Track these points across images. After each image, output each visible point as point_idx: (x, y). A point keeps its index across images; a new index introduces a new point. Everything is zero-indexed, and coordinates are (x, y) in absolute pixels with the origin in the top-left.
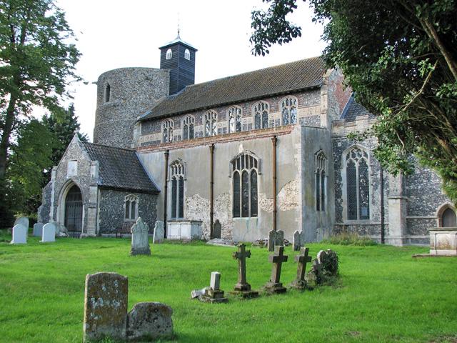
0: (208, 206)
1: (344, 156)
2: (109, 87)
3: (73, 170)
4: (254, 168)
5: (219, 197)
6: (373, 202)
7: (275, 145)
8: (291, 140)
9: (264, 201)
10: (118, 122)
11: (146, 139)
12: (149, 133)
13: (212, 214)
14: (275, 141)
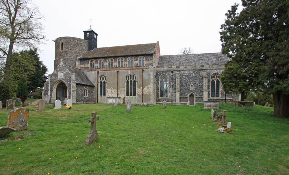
0: (116, 92)
1: (160, 77)
2: (62, 44)
3: (61, 76)
4: (135, 79)
5: (120, 89)
6: (169, 92)
7: (143, 72)
8: (149, 71)
9: (138, 91)
10: (68, 58)
11: (82, 66)
12: (83, 64)
13: (118, 95)
14: (143, 71)
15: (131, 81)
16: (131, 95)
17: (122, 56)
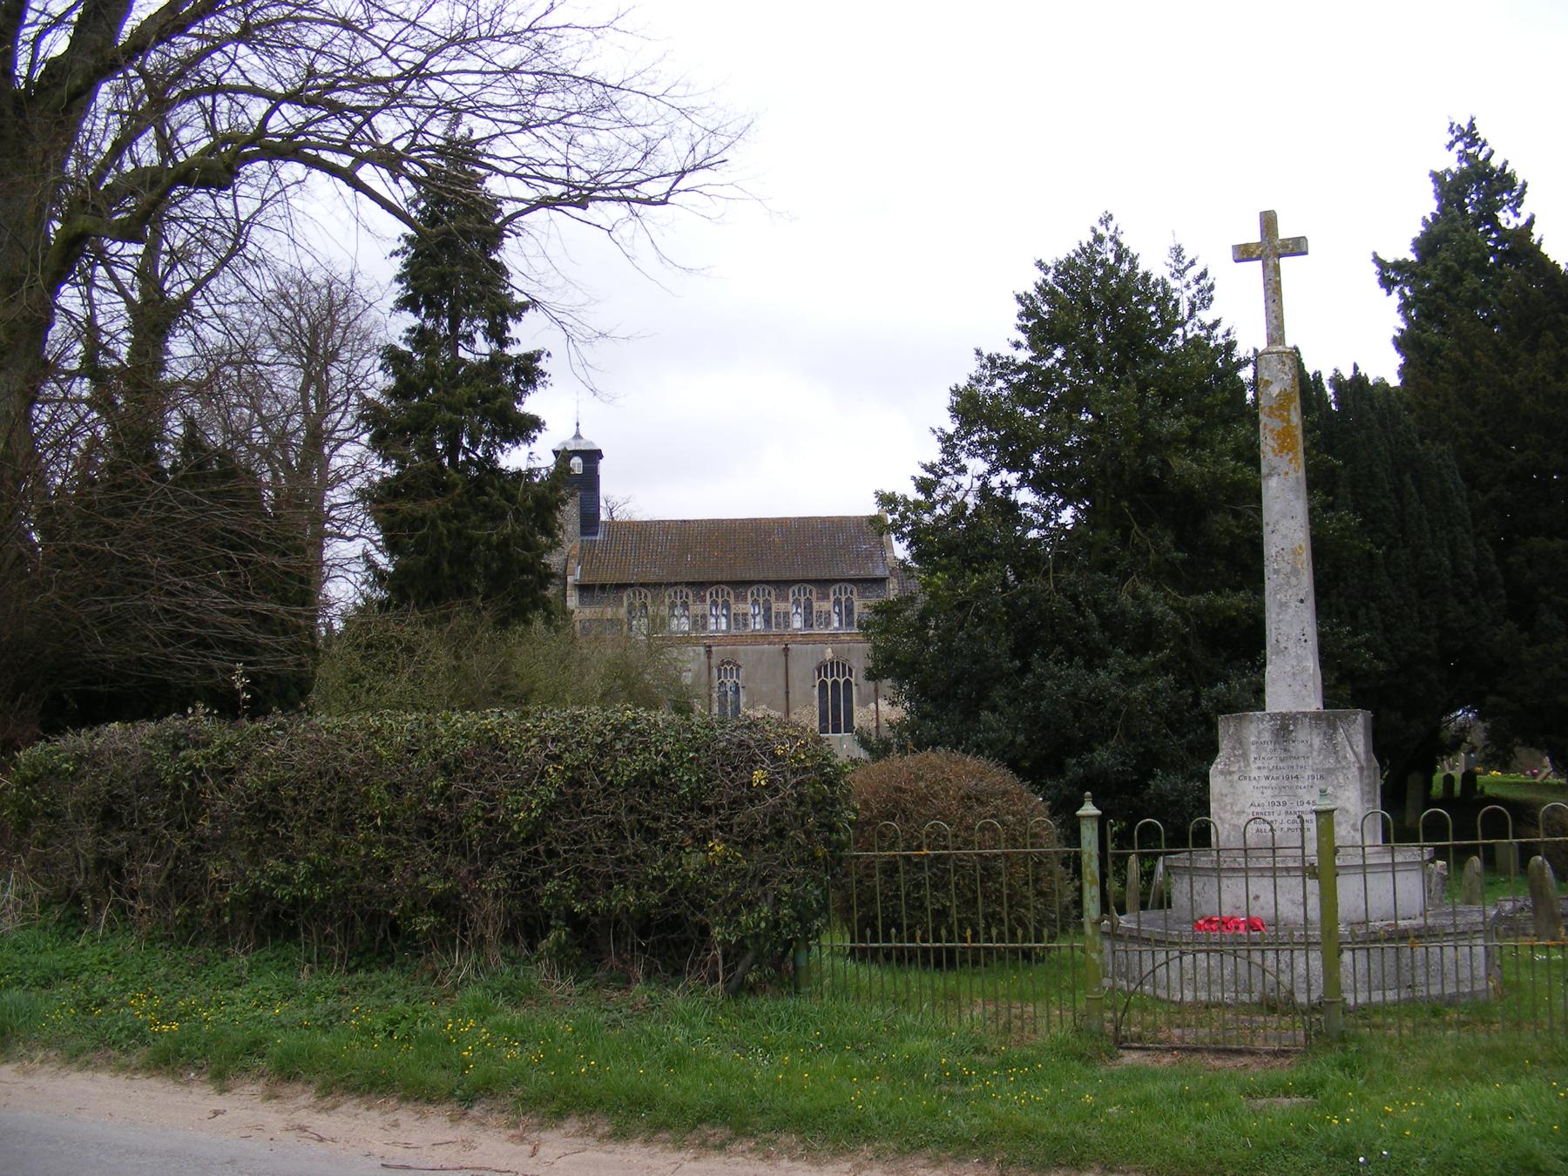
15: (835, 683)
16: (836, 730)
17: (768, 582)
